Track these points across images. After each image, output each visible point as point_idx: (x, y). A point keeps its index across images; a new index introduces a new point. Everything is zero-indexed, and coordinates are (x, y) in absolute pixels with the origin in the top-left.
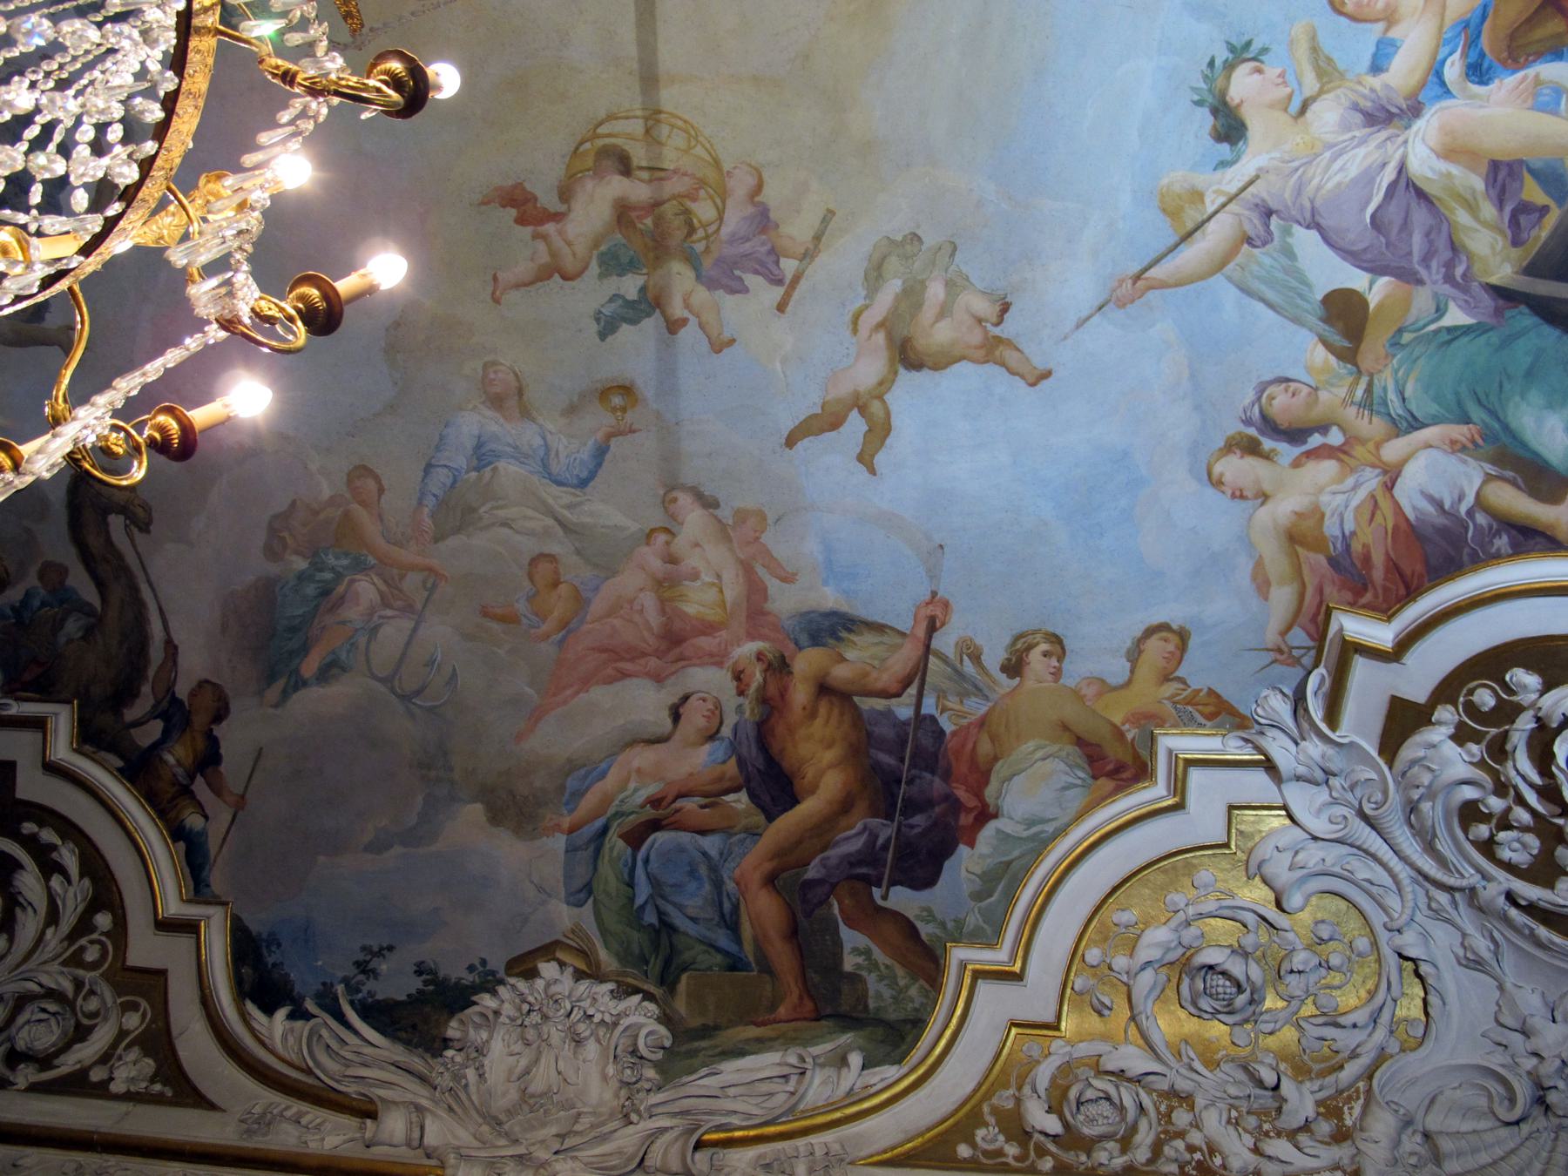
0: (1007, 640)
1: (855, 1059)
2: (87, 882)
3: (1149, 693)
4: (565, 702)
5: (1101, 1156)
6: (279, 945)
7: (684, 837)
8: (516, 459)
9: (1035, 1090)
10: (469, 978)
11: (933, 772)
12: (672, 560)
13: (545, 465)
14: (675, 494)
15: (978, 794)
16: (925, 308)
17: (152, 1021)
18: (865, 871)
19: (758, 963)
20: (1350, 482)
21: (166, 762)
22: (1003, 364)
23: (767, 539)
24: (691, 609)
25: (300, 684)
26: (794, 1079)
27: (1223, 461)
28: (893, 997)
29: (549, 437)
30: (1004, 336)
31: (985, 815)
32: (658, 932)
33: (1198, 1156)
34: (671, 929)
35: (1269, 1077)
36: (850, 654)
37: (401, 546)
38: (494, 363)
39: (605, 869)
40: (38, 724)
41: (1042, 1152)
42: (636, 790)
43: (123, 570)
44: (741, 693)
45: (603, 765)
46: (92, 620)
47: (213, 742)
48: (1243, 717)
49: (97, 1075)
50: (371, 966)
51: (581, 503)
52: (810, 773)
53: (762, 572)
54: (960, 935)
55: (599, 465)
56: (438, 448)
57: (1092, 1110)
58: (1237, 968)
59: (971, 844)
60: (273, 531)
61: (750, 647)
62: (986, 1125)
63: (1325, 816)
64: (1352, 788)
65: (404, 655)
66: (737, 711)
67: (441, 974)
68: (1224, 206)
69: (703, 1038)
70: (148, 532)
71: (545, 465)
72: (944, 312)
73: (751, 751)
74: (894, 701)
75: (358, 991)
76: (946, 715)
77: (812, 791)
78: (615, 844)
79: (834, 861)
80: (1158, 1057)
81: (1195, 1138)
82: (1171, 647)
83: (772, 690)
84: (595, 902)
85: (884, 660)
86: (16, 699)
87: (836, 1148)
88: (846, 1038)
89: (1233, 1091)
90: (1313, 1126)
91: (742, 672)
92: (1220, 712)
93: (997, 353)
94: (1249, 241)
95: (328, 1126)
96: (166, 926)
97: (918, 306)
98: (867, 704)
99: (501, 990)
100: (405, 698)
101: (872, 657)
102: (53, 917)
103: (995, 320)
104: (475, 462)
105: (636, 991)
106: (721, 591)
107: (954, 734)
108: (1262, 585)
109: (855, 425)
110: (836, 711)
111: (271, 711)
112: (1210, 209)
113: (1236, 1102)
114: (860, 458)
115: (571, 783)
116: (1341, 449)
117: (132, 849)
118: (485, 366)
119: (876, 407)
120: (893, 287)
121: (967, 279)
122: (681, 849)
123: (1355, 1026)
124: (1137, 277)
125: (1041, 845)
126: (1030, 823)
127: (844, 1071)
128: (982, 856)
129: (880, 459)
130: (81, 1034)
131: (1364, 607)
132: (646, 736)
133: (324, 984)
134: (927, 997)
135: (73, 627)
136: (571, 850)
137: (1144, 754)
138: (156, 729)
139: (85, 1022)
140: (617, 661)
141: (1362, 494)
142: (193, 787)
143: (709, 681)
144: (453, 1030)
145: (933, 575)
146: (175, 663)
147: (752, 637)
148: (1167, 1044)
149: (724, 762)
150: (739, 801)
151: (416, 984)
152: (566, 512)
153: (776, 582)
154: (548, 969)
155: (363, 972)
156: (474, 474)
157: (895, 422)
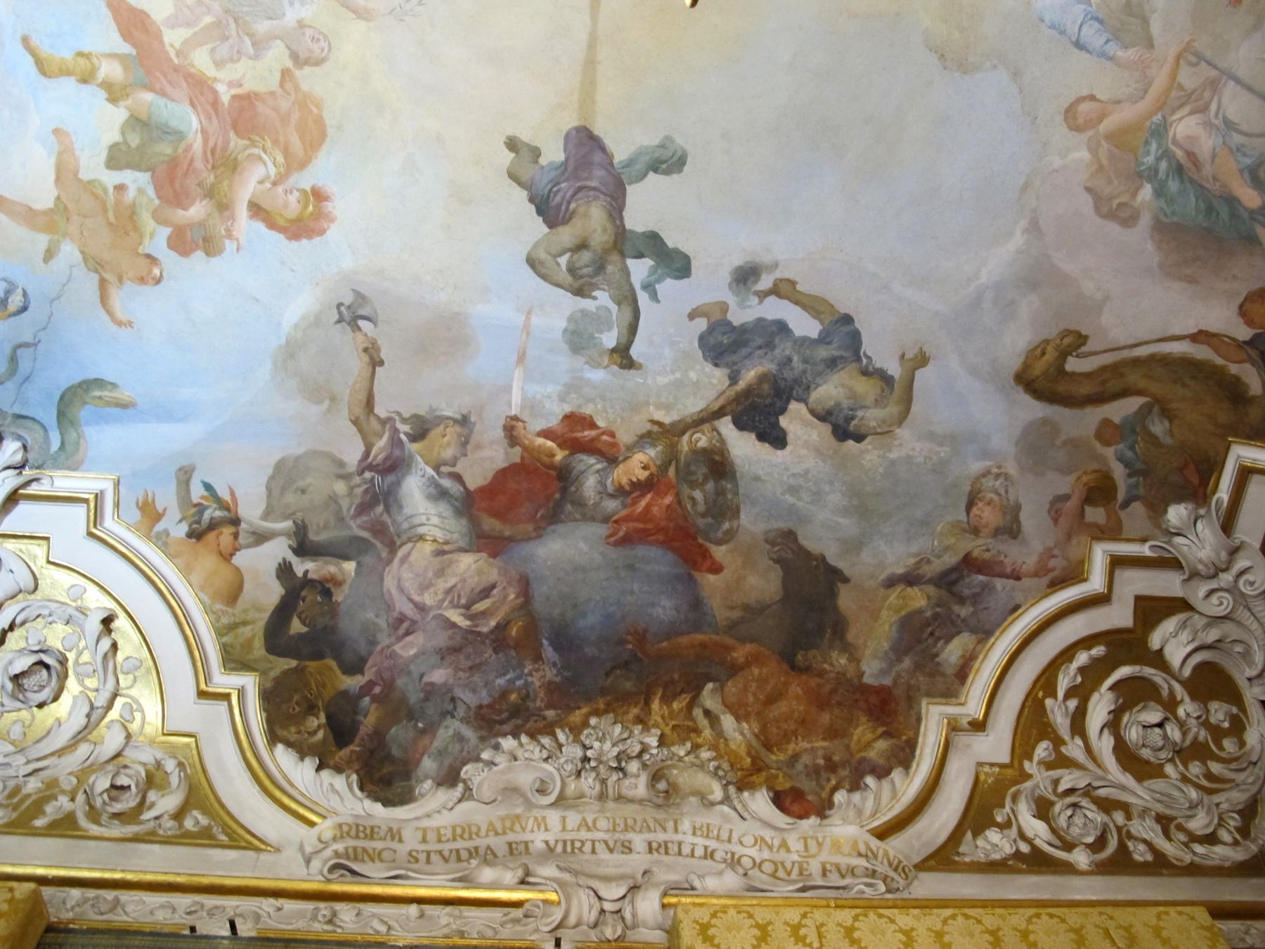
37: (1150, 84)
43: (1114, 369)
46: (1156, 409)
56: (1063, 33)
60: (1111, 215)
70: (1086, 337)
86: (1214, 492)
135: (1158, 427)
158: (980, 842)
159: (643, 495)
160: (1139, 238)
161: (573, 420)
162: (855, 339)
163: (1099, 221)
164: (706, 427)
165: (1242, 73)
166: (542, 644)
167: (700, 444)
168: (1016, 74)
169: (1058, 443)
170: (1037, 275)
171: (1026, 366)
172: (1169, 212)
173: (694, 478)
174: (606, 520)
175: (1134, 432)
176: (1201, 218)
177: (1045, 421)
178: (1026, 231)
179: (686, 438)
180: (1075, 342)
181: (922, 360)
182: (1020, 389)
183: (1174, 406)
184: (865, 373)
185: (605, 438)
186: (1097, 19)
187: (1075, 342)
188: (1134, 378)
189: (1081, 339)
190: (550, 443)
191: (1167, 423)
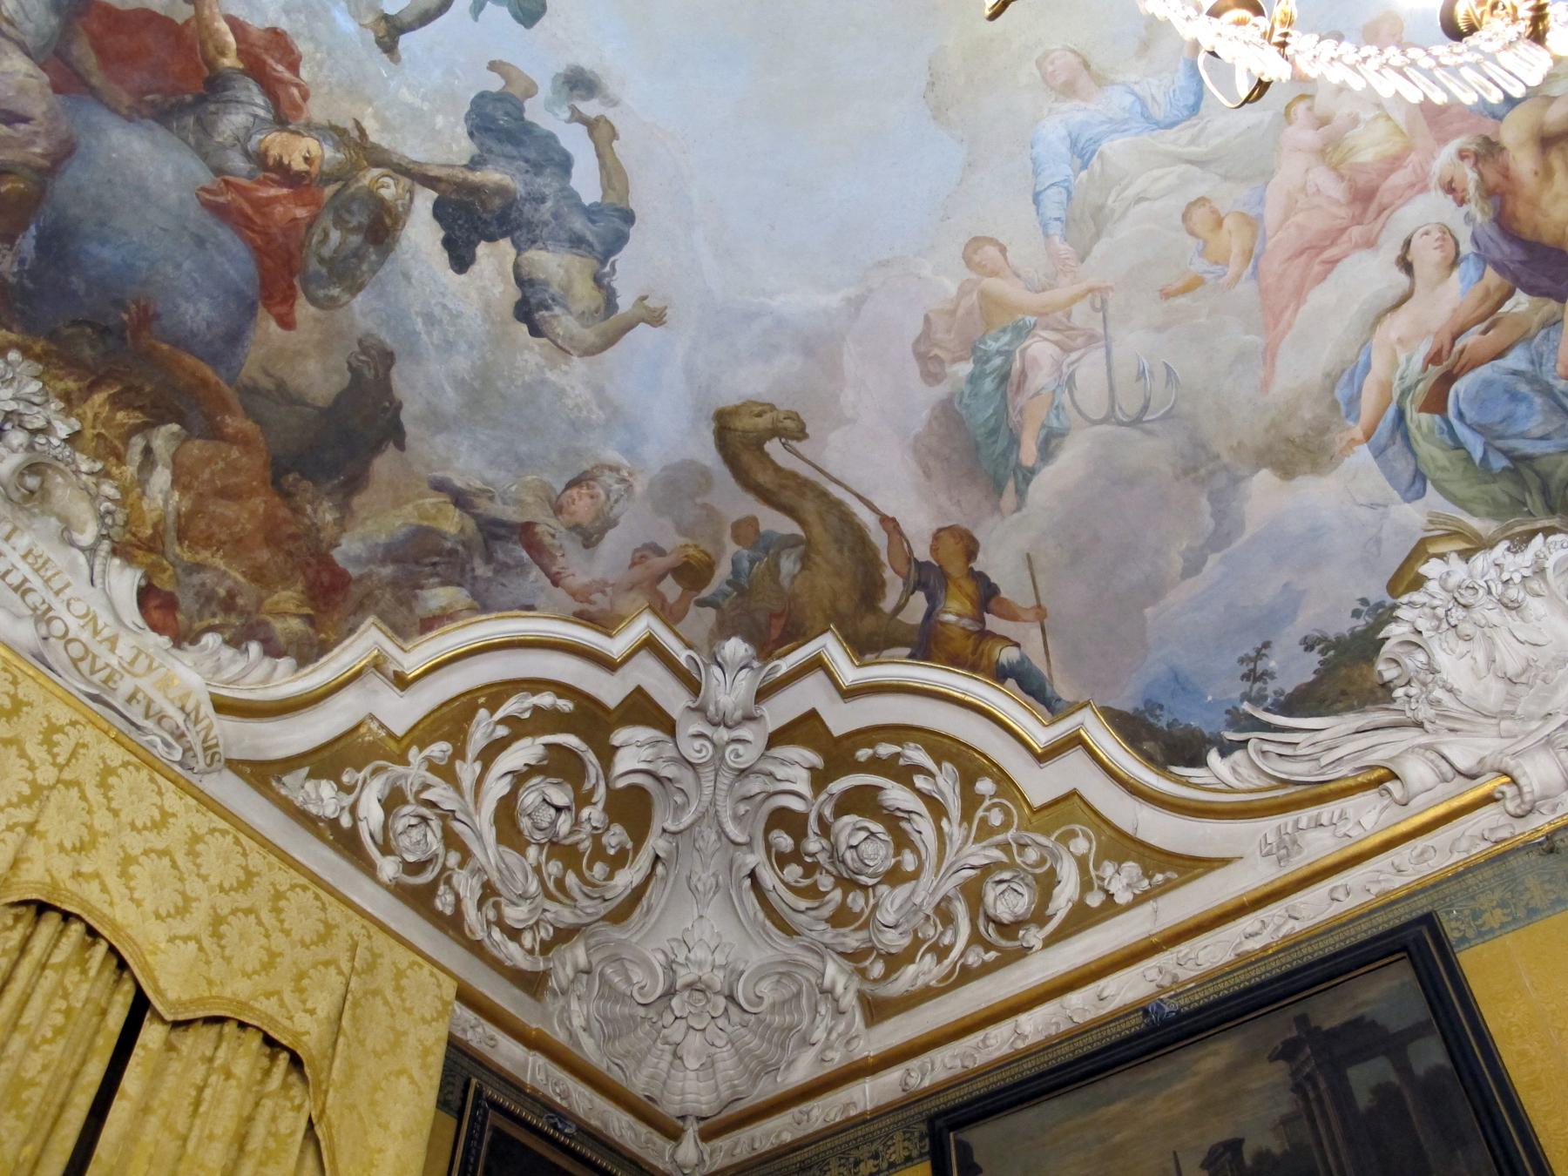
2: (947, 766)
4: (1290, 326)
6: (1161, 707)
7: (1485, 371)
8: (1115, 131)
10: (1360, 624)
12: (1323, 122)
13: (1147, 117)
17: (1098, 836)
21: (944, 624)
25: (1028, 474)
29: (1137, 88)
34: (1528, 459)
37: (1052, 287)
38: (1046, 55)
39: (1424, 448)
40: (818, 664)
42: (1409, 360)
43: (804, 485)
44: (1461, 202)
45: (1362, 359)
46: (802, 547)
47: (980, 578)
49: (1095, 900)
50: (1259, 670)
51: (1202, 130)
56: (1036, 173)
60: (922, 357)
61: (1448, 151)
65: (1112, 389)
66: (1467, 221)
67: (1332, 637)
70: (806, 436)
71: (1147, 117)
73: (1504, 250)
75: (1266, 697)
78: (1421, 421)
83: (1492, 177)
84: (1434, 482)
91: (1451, 182)
95: (1350, 813)
96: (1044, 757)
99: (1398, 613)
100: (1136, 422)
102: (937, 809)
104: (1078, 162)
105: (1534, 533)
106: (1389, 118)
111: (1016, 515)
115: (1340, 394)
117: (973, 715)
118: (1039, 64)
122: (1488, 384)
130: (1047, 884)
133: (1228, 712)
135: (788, 565)
136: (1379, 453)
138: (919, 602)
139: (1038, 871)
140: (1321, 254)
142: (988, 627)
144: (1389, 673)
146: (901, 534)
147: (1443, 141)
149: (1481, 277)
150: (1518, 304)
151: (1314, 659)
152: (1193, 149)
154: (1431, 568)
155: (1256, 679)
156: (1084, 174)
158: (309, 785)
159: (280, 184)
160: (926, 398)
161: (278, 40)
162: (620, 240)
163: (909, 349)
164: (405, 182)
165: (1116, 352)
166: (26, 228)
167: (385, 193)
168: (970, 165)
169: (699, 501)
170: (819, 347)
171: (735, 412)
172: (966, 400)
173: (347, 217)
174: (218, 171)
175: (766, 550)
176: (983, 430)
177: (705, 474)
178: (849, 300)
179: (376, 172)
180: (793, 431)
181: (656, 318)
182: (713, 425)
183: (818, 559)
184: (598, 280)
185: (295, 91)
186: (1069, 193)
187: (793, 431)
188: (809, 507)
189: (801, 434)
190: (231, 39)
191: (798, 567)
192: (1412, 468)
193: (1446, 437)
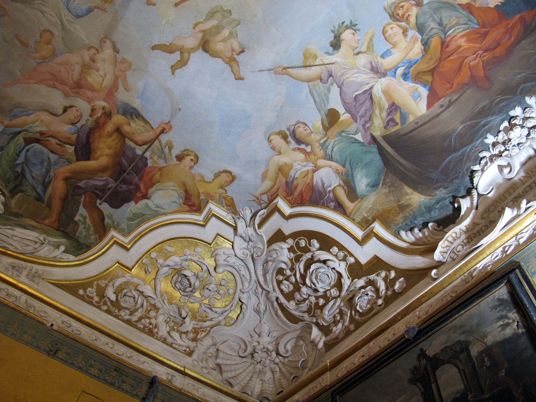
0: (183, 149)
1: (62, 248)
3: (214, 189)
4: (29, 84)
5: (122, 313)
7: (45, 150)
9: (113, 285)
11: (137, 175)
12: (93, 60)
14: (106, 40)
15: (147, 189)
16: (219, 35)
18: (98, 193)
19: (47, 202)
20: (305, 164)
22: (231, 68)
23: (128, 73)
24: (90, 79)
26: (38, 244)
27: (275, 136)
28: (85, 235)
30: (237, 59)
31: (145, 196)
32: (18, 175)
33: (151, 326)
35: (184, 314)
36: (132, 124)
41: (105, 303)
42: (37, 126)
44: (91, 116)
45: (30, 112)
48: (236, 211)
51: (73, 22)
52: (99, 153)
53: (120, 83)
54: (117, 228)
55: (87, 14)
57: (128, 299)
58: (193, 280)
59: (136, 203)
61: (102, 103)
62: (92, 287)
63: (242, 251)
64: (254, 248)
66: (86, 120)
68: (321, 65)
69: (15, 217)
72: (224, 40)
73: (83, 136)
74: (138, 147)
76: (151, 160)
77: (96, 159)
78: (20, 139)
79: (90, 185)
80: (156, 294)
81: (153, 321)
82: (228, 179)
83: (102, 121)
85: (142, 132)
87: (40, 272)
88: (63, 240)
89: (171, 313)
90: (188, 334)
92: (231, 206)
93: (232, 63)
94: (321, 79)
97: (218, 33)
98: (129, 142)
101: (139, 129)
103: (237, 53)
106: (103, 80)
107: (150, 167)
108: (264, 177)
109: (176, 56)
110: (118, 139)
112: (316, 63)
113: (171, 317)
114: (172, 67)
115: (15, 111)
116: (308, 153)
119: (186, 55)
120: (214, 22)
121: (237, 35)
122: (42, 153)
123: (216, 312)
124: (285, 68)
125: (157, 214)
126: (158, 206)
127: (57, 250)
128: (137, 208)
129: (178, 71)
131: (287, 200)
132: (51, 111)
134: (96, 241)
137: (203, 205)
140: (56, 81)
141: (306, 169)
143: (83, 106)
145: (172, 116)
147: (105, 101)
148: (161, 291)
149: (73, 134)
152: (66, 22)
153: (123, 88)
157: (189, 63)
192: (3, 145)
193: (19, 150)
